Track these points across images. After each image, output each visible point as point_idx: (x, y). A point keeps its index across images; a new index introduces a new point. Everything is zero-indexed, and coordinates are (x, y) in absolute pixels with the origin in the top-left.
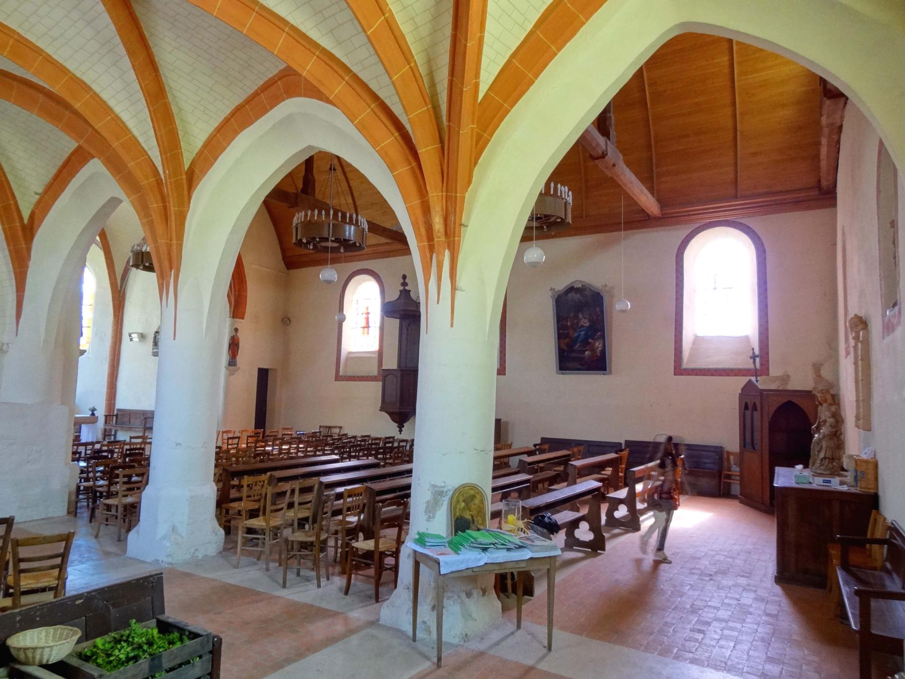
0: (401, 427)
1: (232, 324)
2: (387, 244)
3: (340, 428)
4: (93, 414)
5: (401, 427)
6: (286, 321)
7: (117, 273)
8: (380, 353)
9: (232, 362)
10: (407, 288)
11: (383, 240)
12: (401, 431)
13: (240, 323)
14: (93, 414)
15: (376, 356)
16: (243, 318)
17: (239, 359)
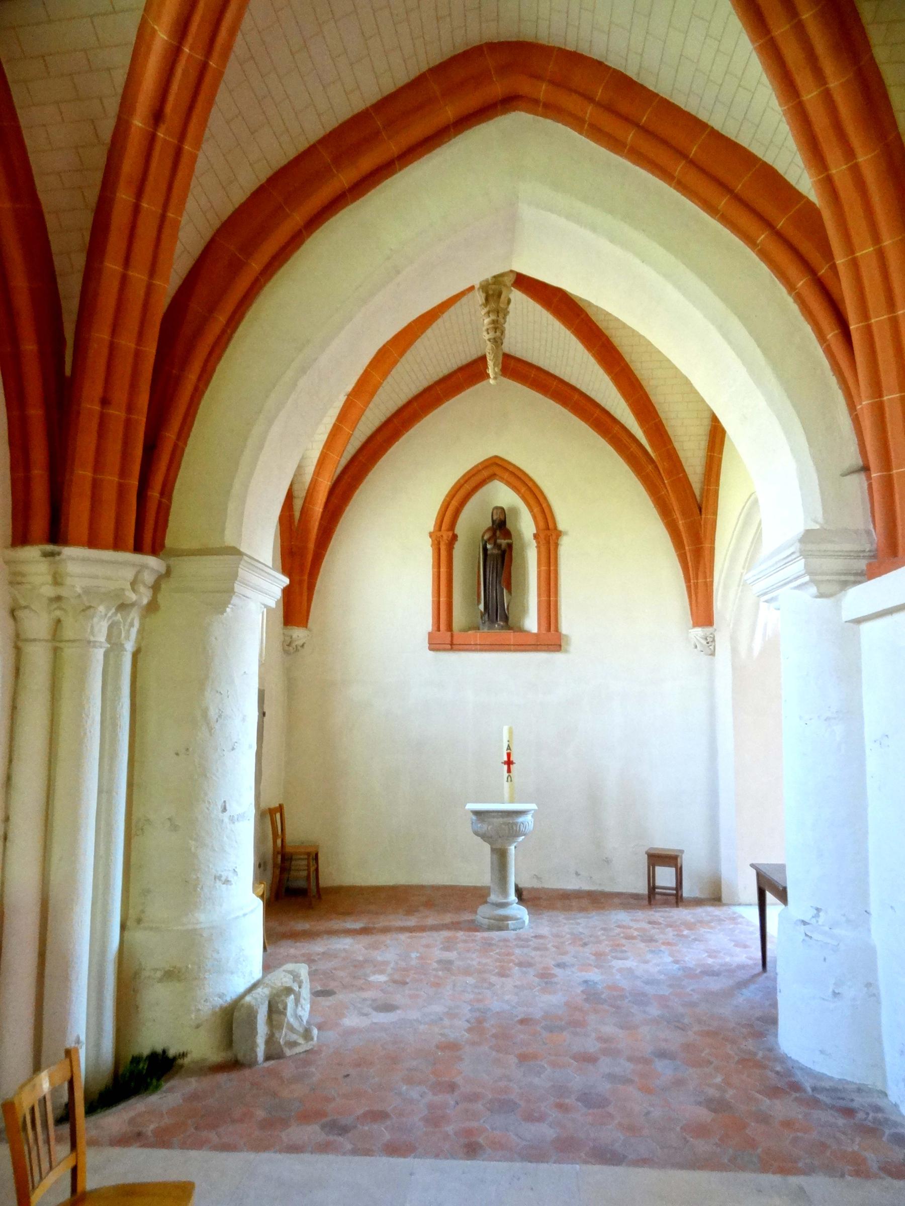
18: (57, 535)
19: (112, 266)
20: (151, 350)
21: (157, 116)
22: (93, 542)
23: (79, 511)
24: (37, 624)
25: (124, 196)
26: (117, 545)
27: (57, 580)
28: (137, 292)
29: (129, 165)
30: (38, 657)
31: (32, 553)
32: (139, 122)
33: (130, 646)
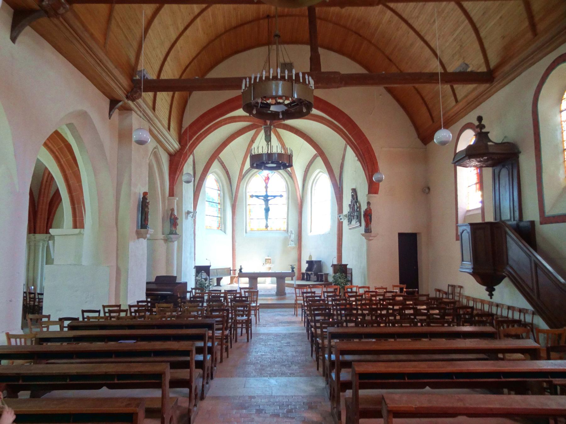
0: (491, 290)
1: (368, 199)
2: (475, 89)
3: (461, 287)
4: (293, 271)
5: (491, 290)
6: (427, 190)
7: (336, 176)
8: (483, 209)
9: (368, 230)
10: (484, 130)
11: (470, 87)
12: (491, 295)
13: (375, 198)
14: (293, 271)
15: (480, 211)
16: (376, 192)
17: (373, 225)
18: (35, 233)
19: (41, 198)
20: (48, 207)
21: (47, 181)
22: (40, 233)
23: (38, 229)
24: (32, 244)
25: (43, 190)
26: (43, 233)
27: (35, 238)
28: (45, 200)
29: (43, 187)
30: (32, 248)
31: (31, 235)
32: (44, 183)
33: (46, 246)
